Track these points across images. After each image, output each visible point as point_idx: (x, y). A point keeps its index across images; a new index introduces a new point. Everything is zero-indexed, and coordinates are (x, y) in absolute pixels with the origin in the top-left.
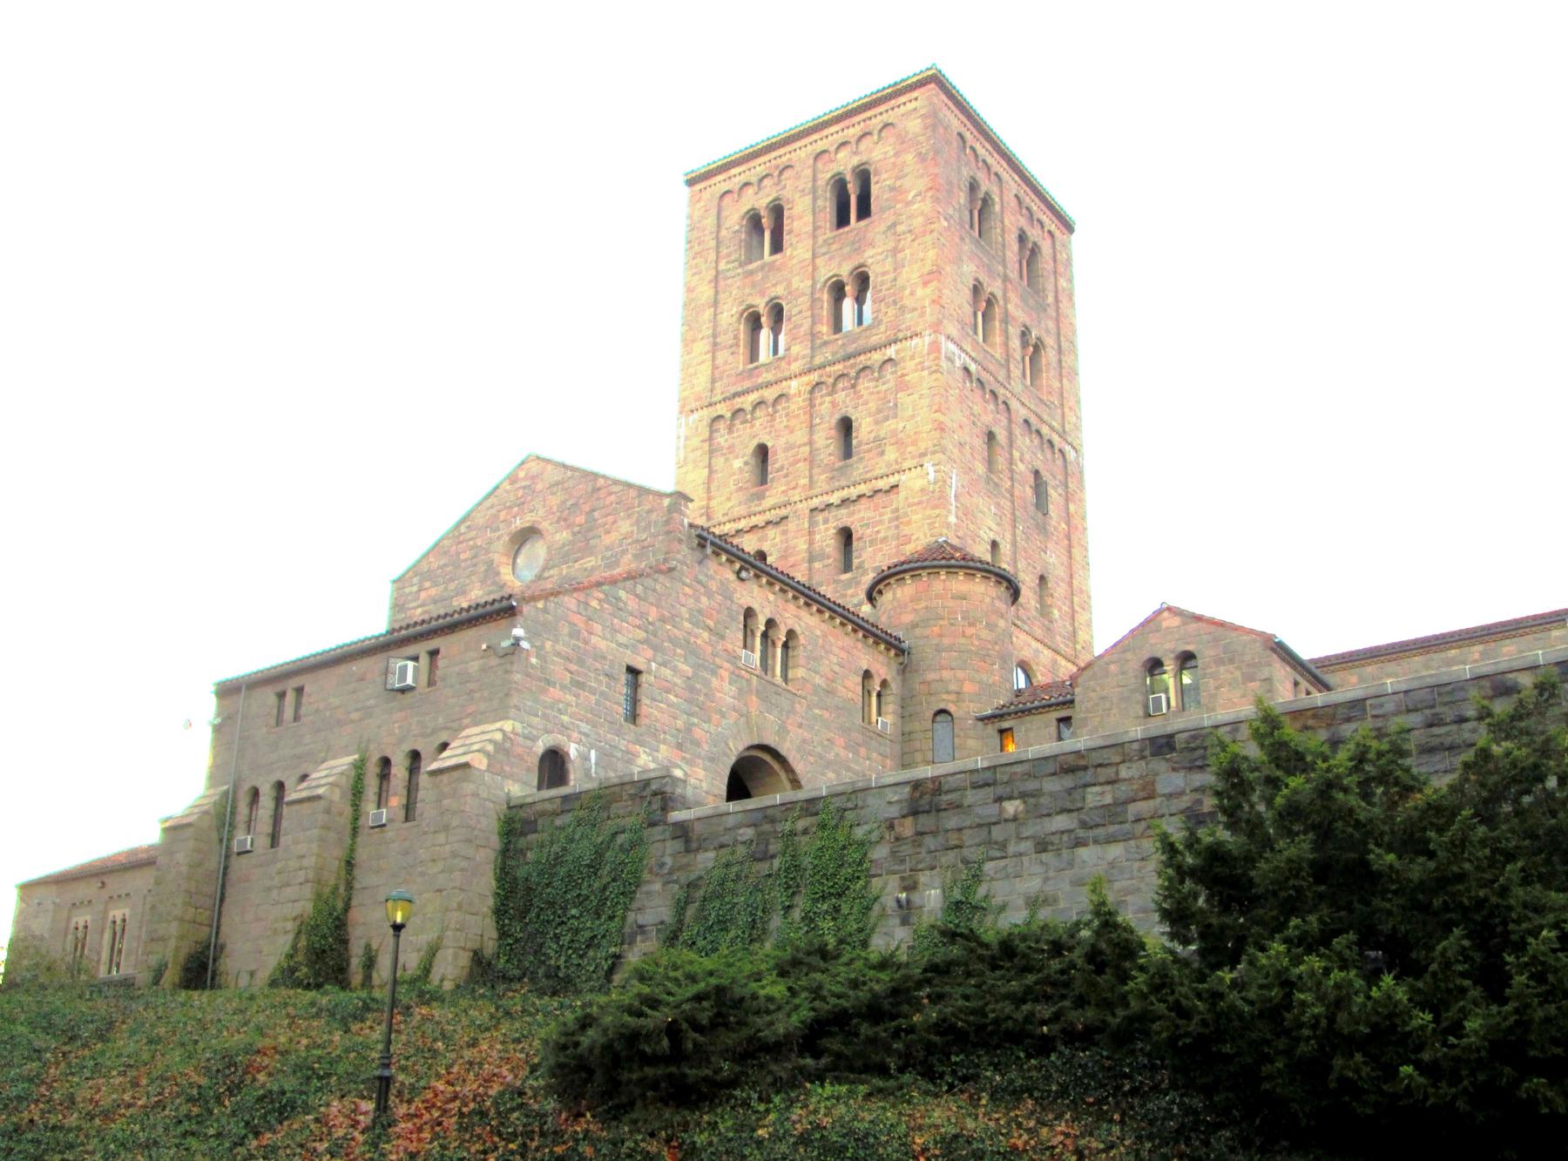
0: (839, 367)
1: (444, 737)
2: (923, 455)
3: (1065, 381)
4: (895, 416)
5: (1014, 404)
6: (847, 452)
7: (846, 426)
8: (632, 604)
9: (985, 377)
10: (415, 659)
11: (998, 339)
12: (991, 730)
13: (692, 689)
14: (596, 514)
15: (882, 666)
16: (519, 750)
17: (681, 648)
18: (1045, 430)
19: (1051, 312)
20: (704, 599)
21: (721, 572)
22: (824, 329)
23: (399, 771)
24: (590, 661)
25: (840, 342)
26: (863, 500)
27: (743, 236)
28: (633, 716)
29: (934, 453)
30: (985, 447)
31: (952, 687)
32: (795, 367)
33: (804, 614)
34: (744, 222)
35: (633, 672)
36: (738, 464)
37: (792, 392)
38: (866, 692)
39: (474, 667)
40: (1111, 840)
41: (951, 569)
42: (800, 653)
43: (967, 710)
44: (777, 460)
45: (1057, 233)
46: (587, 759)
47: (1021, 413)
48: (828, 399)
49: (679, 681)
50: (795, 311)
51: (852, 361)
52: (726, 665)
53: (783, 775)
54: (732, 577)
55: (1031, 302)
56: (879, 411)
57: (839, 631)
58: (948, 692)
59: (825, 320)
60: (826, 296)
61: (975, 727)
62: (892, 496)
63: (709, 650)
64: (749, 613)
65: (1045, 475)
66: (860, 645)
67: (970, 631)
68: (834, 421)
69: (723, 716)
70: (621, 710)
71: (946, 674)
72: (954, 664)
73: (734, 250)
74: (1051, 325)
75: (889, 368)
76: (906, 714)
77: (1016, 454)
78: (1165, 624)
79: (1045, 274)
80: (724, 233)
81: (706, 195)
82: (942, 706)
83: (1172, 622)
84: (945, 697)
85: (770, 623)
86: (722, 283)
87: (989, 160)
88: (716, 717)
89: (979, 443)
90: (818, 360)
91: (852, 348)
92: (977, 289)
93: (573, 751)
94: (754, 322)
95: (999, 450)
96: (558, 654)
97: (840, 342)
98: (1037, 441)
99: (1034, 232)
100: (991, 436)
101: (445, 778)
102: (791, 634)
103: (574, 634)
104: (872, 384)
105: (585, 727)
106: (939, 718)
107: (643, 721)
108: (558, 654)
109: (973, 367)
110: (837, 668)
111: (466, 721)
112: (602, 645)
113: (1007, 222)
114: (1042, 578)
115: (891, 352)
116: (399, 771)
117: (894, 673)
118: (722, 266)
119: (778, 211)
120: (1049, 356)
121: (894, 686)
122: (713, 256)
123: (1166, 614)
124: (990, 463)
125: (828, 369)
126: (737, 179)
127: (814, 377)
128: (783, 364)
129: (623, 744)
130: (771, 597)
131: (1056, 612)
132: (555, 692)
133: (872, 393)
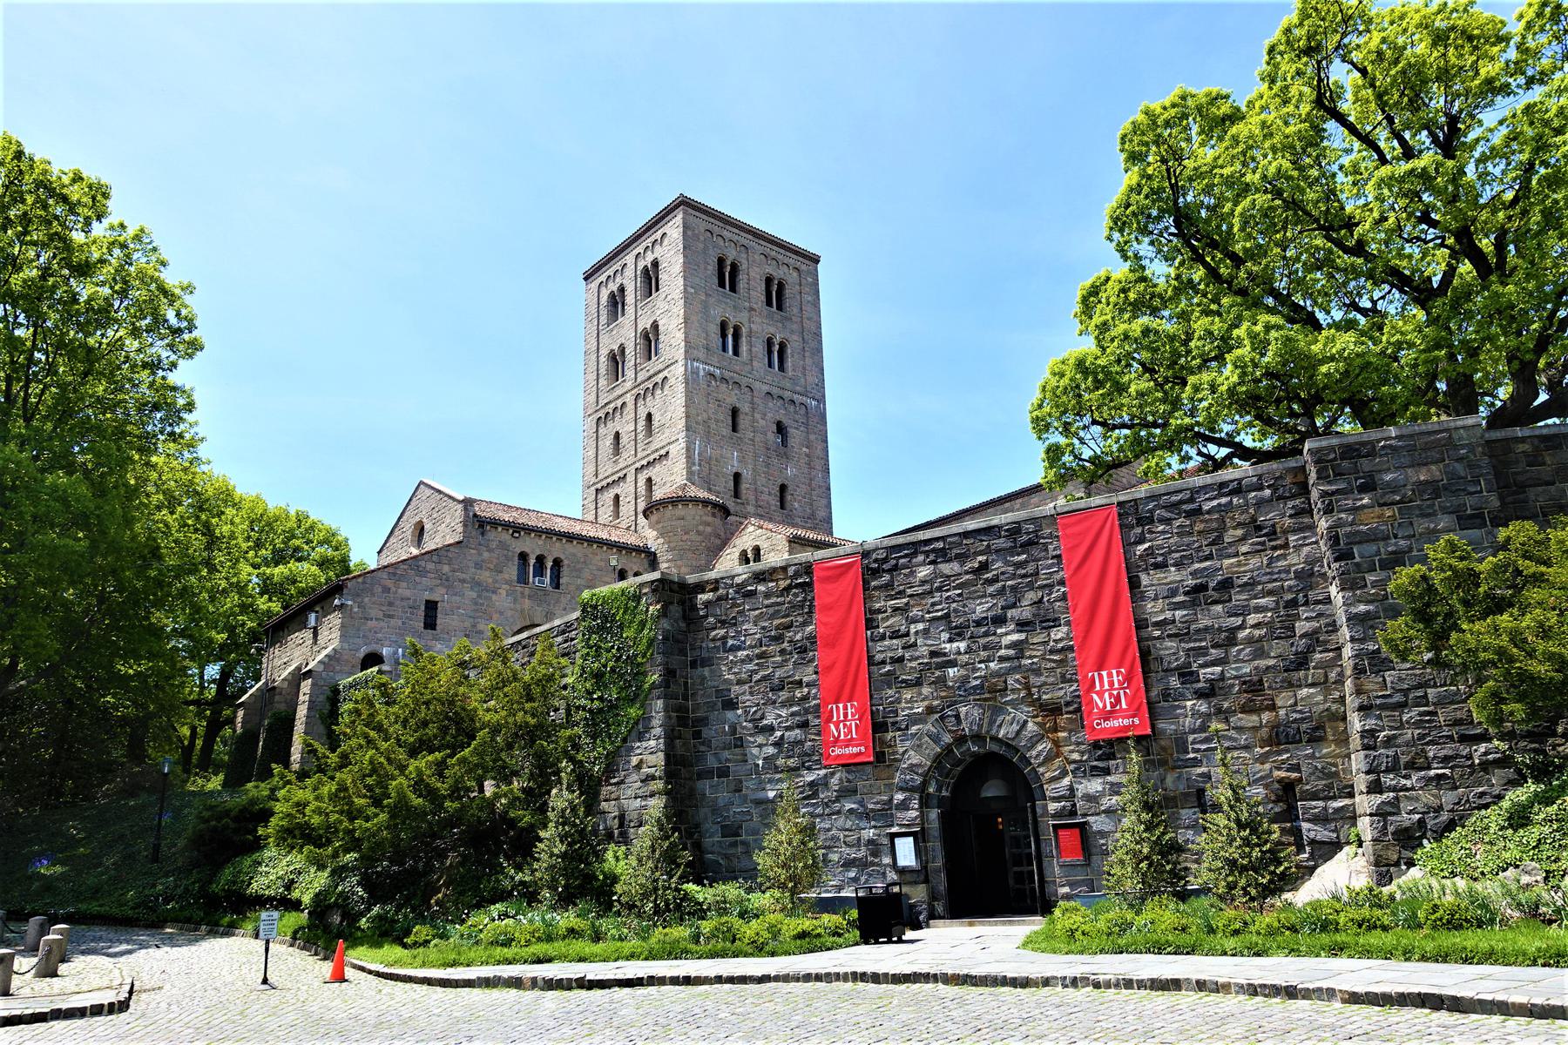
5: (757, 385)
7: (649, 416)
8: (430, 566)
9: (727, 374)
11: (744, 348)
18: (787, 394)
20: (486, 555)
36: (608, 443)
44: (624, 440)
45: (804, 267)
46: (396, 653)
63: (490, 580)
65: (786, 421)
67: (685, 538)
69: (501, 613)
73: (604, 319)
77: (757, 416)
85: (540, 560)
87: (735, 238)
90: (639, 380)
91: (652, 372)
92: (723, 326)
95: (741, 417)
99: (781, 272)
100: (735, 412)
102: (557, 563)
103: (386, 590)
112: (408, 593)
113: (752, 274)
114: (783, 488)
115: (665, 373)
119: (622, 289)
130: (540, 543)
131: (796, 504)
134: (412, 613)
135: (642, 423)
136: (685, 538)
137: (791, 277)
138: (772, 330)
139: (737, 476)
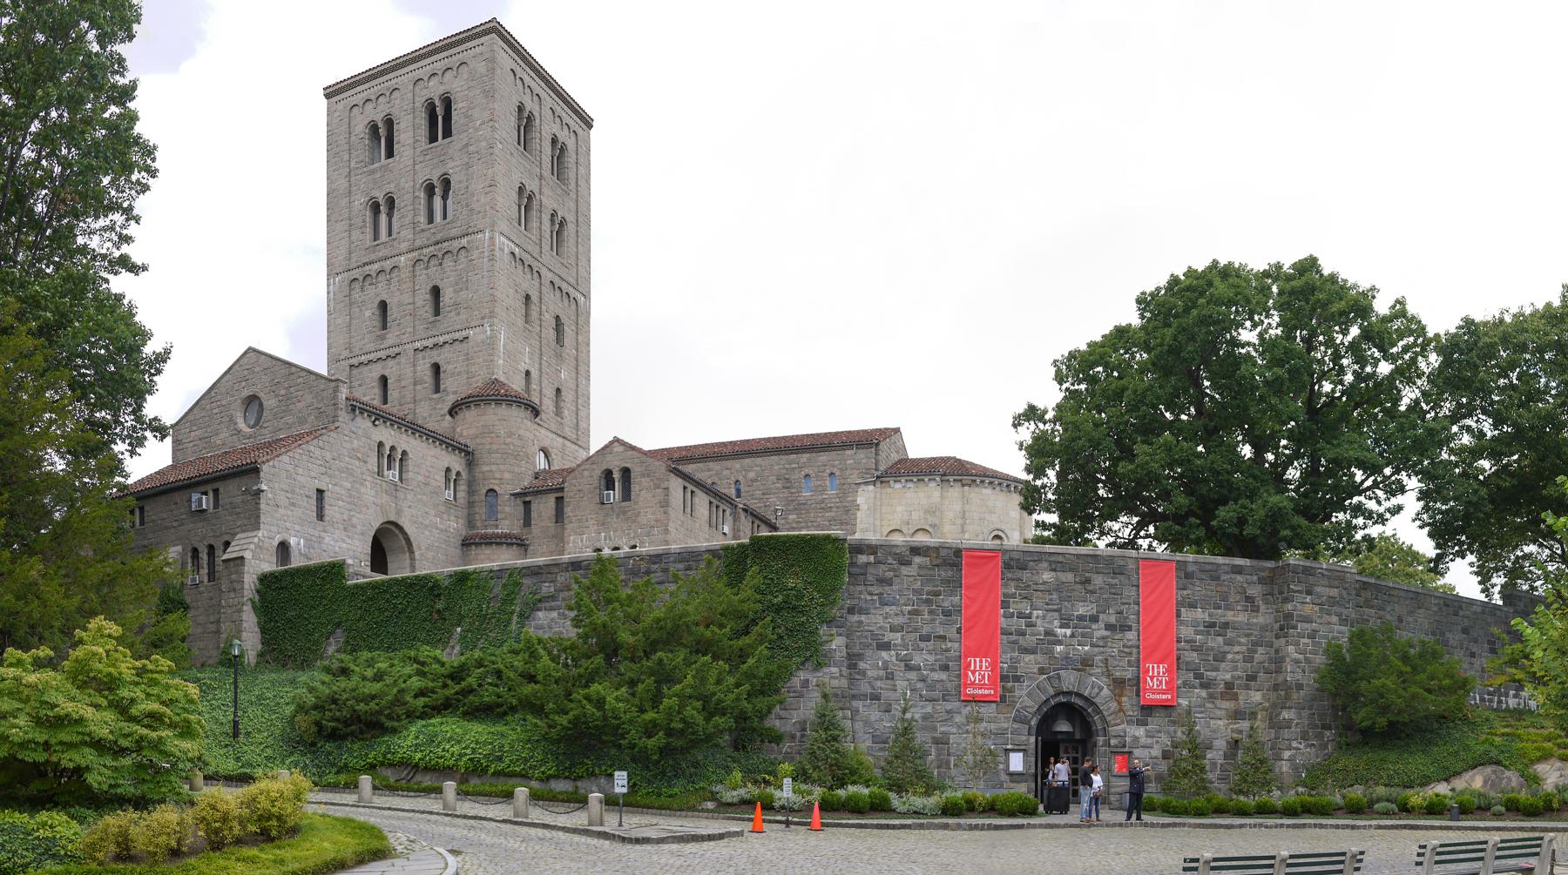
0: (431, 249)
1: (226, 538)
2: (483, 318)
3: (580, 246)
4: (467, 289)
5: (544, 271)
6: (437, 312)
7: (436, 292)
8: (318, 452)
9: (525, 256)
10: (205, 493)
11: (534, 224)
12: (519, 501)
13: (350, 496)
14: (292, 390)
15: (456, 463)
16: (267, 545)
17: (344, 472)
19: (573, 195)
21: (364, 423)
22: (422, 219)
23: (204, 556)
24: (297, 490)
25: (432, 231)
26: (447, 345)
27: (367, 142)
28: (320, 516)
29: (491, 317)
30: (524, 306)
31: (497, 476)
32: (404, 246)
33: (411, 439)
34: (367, 131)
35: (320, 492)
37: (402, 265)
38: (447, 479)
39: (239, 500)
40: (552, 609)
41: (498, 402)
42: (410, 464)
43: (505, 490)
46: (299, 544)
47: (547, 276)
48: (425, 272)
49: (343, 492)
50: (402, 204)
51: (440, 245)
52: (369, 478)
53: (401, 536)
54: (370, 425)
55: (559, 191)
56: (457, 284)
57: (432, 446)
58: (495, 479)
59: (422, 213)
60: (422, 195)
61: (510, 500)
62: (464, 344)
64: (381, 445)
66: (444, 452)
67: (508, 440)
68: (429, 288)
70: (315, 515)
71: (494, 468)
72: (498, 462)
74: (572, 205)
75: (463, 252)
76: (471, 492)
78: (615, 449)
79: (570, 166)
80: (353, 138)
81: (340, 106)
82: (491, 487)
83: (618, 448)
84: (493, 481)
85: (393, 448)
86: (353, 179)
88: (364, 509)
89: (519, 304)
90: (418, 243)
91: (439, 237)
93: (293, 541)
94: (376, 208)
95: (533, 307)
96: (282, 490)
97: (432, 231)
98: (558, 293)
100: (528, 297)
101: (232, 564)
102: (404, 453)
104: (452, 264)
105: (297, 527)
106: (489, 494)
107: (327, 518)
108: (282, 490)
109: (517, 251)
110: (431, 469)
111: (237, 530)
116: (204, 556)
117: (464, 466)
118: (353, 164)
120: (570, 228)
121: (464, 475)
122: (346, 157)
123: (616, 444)
124: (527, 315)
125: (424, 250)
126: (362, 95)
127: (415, 254)
128: (395, 243)
129: (316, 533)
132: (281, 511)
133: (452, 271)
134: (308, 502)
135: (424, 297)
136: (508, 440)
137: (571, 144)
138: (555, 206)
139: (528, 373)
